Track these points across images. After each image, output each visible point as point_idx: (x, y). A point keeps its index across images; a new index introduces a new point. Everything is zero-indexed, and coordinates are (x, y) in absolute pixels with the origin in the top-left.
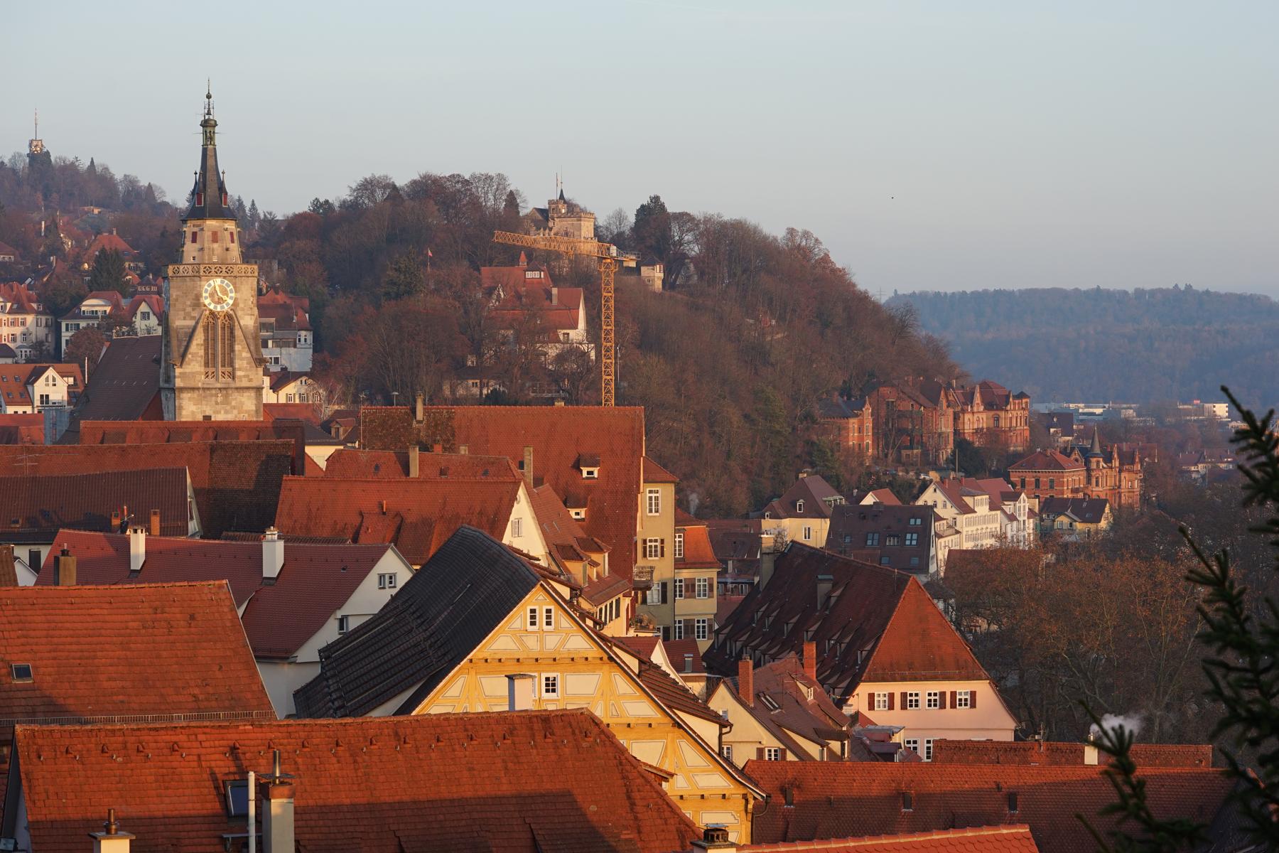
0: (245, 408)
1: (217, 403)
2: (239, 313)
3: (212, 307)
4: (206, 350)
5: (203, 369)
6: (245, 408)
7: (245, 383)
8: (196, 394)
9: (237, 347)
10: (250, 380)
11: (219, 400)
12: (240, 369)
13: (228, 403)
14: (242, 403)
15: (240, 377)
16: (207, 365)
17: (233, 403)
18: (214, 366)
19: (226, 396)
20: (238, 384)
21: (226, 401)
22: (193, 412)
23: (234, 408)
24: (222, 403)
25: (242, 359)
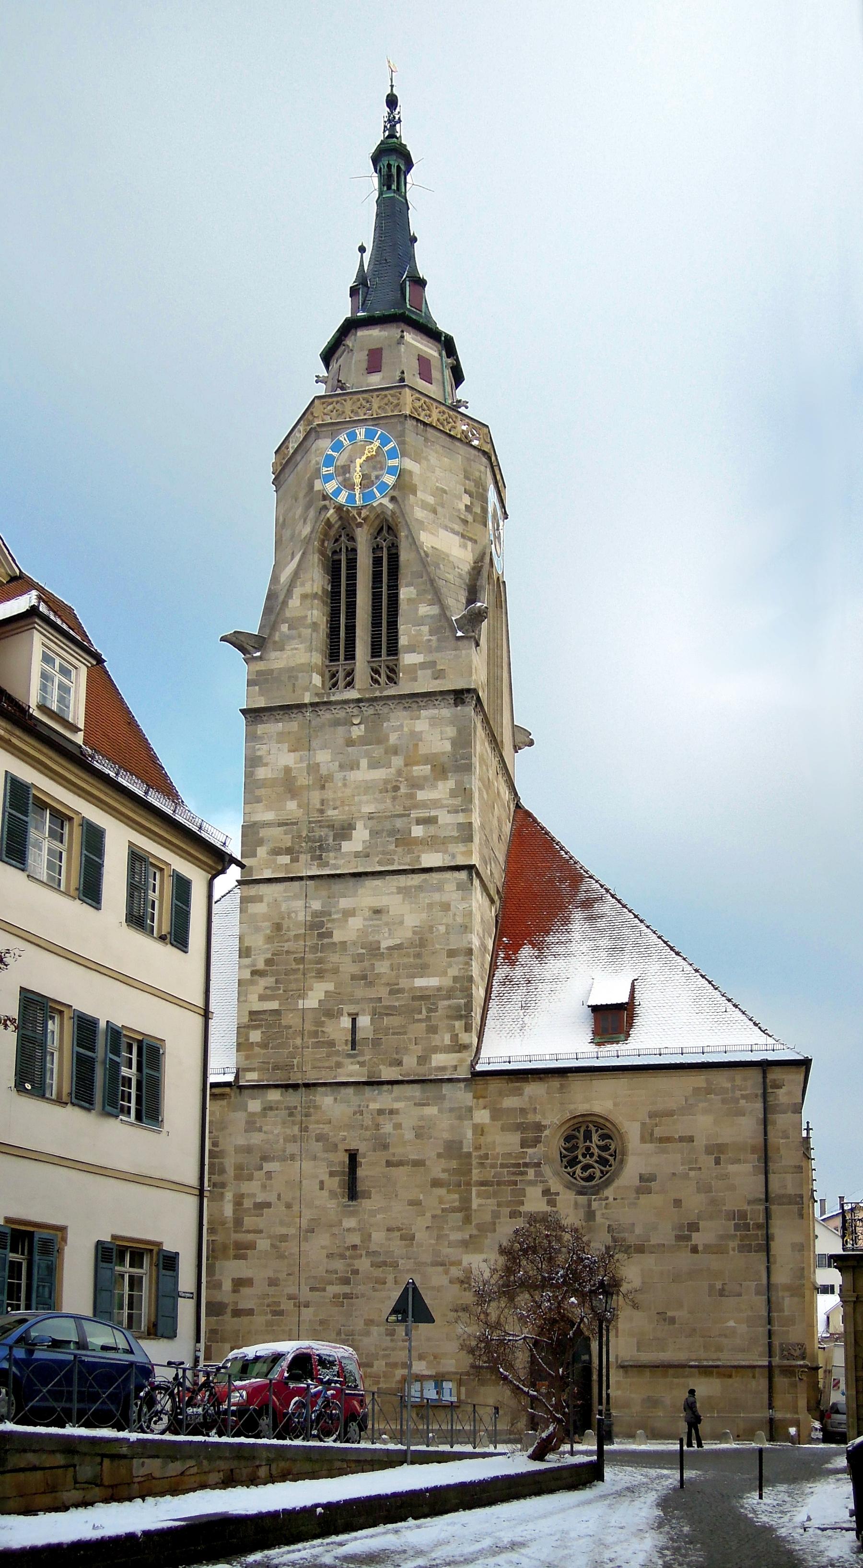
0: (423, 750)
1: (350, 743)
2: (419, 513)
3: (342, 499)
4: (334, 616)
5: (317, 659)
6: (423, 750)
7: (425, 684)
8: (292, 725)
9: (405, 593)
10: (439, 675)
11: (357, 732)
12: (412, 649)
13: (379, 742)
14: (416, 737)
15: (413, 669)
16: (333, 656)
17: (393, 738)
18: (351, 656)
19: (374, 724)
20: (405, 687)
21: (375, 737)
22: (287, 770)
23: (395, 751)
24: (364, 741)
25: (420, 622)
